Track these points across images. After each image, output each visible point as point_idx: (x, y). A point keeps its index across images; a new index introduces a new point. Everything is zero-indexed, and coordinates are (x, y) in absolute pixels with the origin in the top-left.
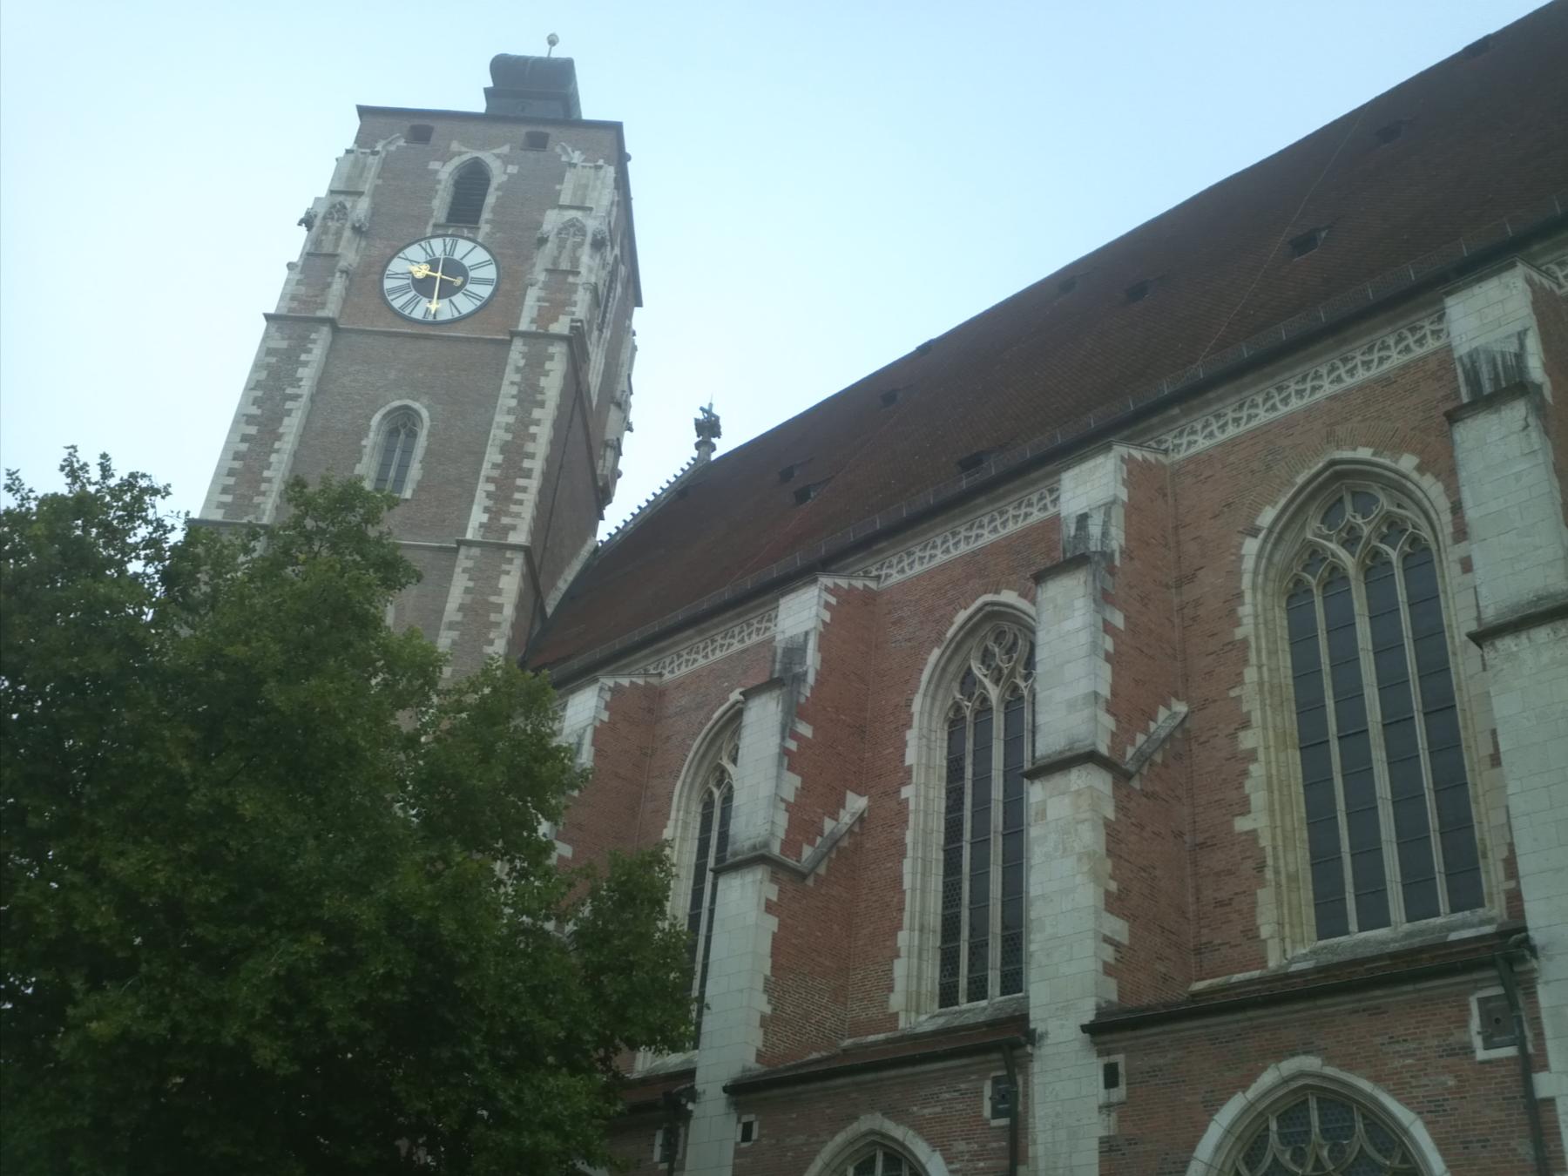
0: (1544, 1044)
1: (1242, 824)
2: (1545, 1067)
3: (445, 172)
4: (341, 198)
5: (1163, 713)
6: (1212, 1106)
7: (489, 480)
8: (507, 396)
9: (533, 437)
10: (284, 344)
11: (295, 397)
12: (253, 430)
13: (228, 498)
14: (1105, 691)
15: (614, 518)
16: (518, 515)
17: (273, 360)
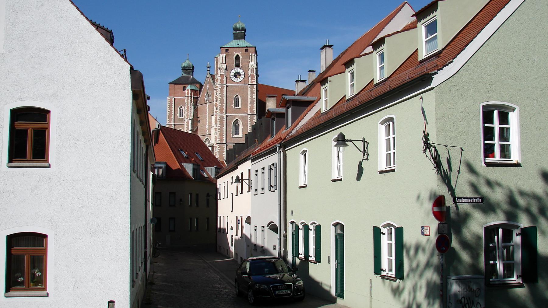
8: (249, 93)
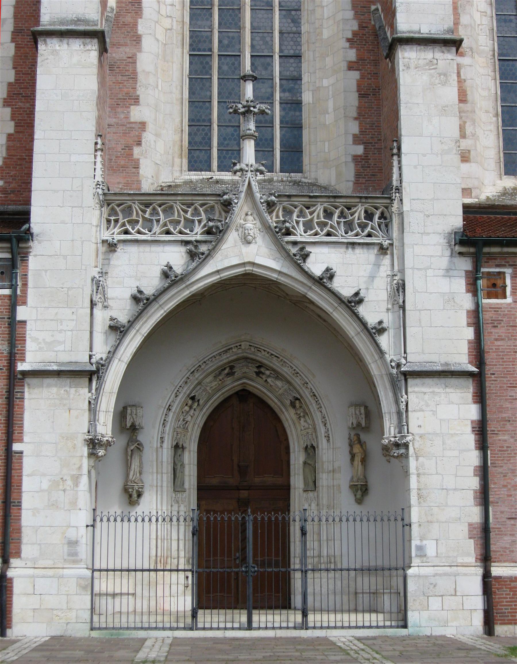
0: (27, 290)
2: (25, 303)
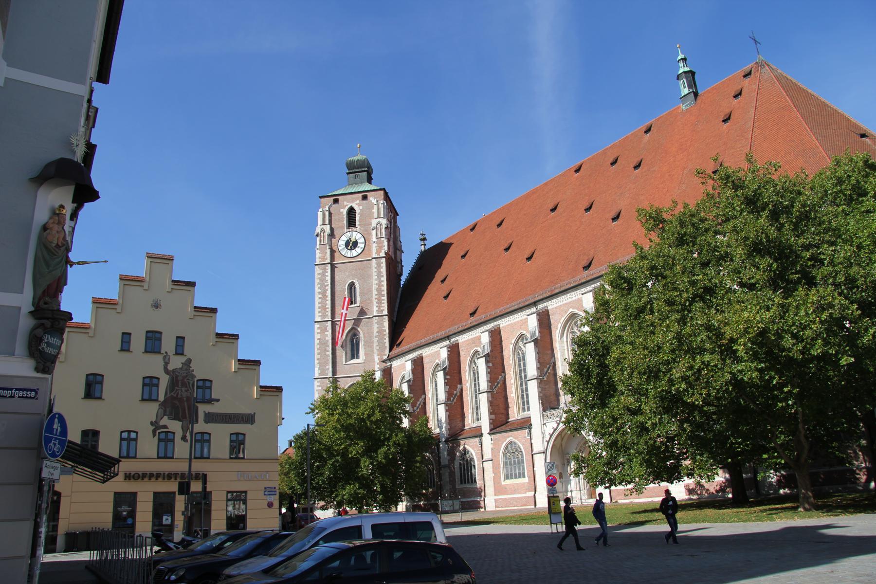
1: (512, 395)
3: (345, 211)
4: (323, 226)
5: (500, 377)
6: (502, 444)
7: (376, 299)
9: (383, 285)
10: (321, 271)
11: (327, 285)
12: (321, 296)
13: (320, 314)
14: (489, 379)
15: (403, 279)
16: (384, 307)
17: (320, 276)
